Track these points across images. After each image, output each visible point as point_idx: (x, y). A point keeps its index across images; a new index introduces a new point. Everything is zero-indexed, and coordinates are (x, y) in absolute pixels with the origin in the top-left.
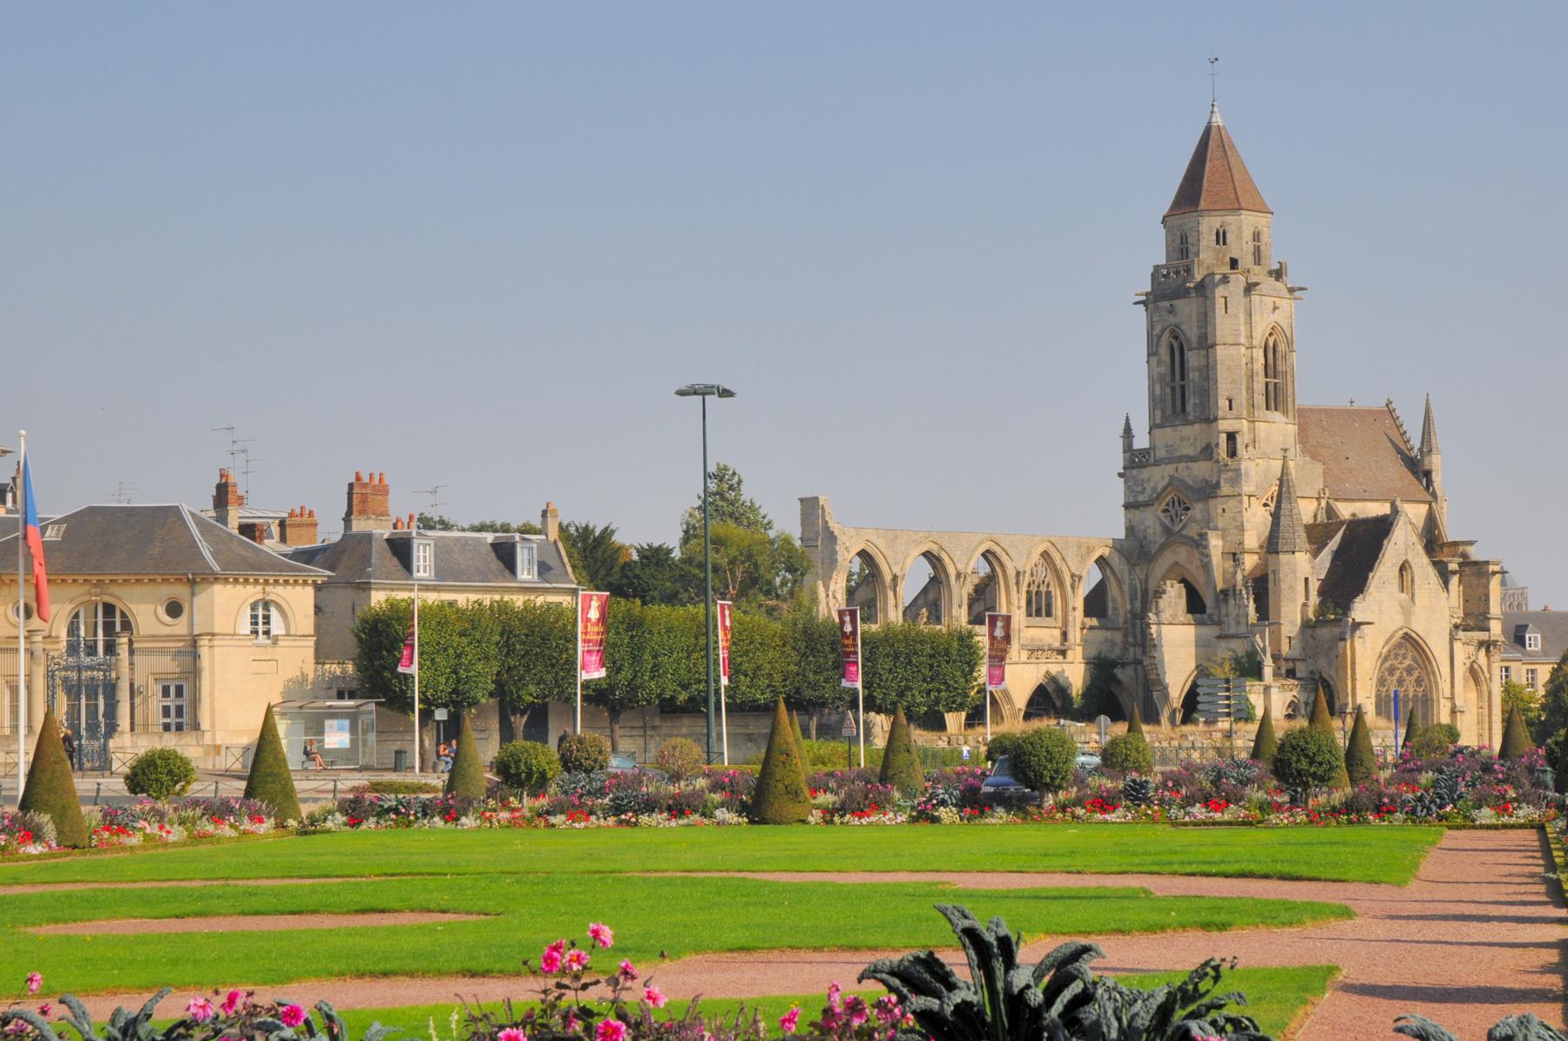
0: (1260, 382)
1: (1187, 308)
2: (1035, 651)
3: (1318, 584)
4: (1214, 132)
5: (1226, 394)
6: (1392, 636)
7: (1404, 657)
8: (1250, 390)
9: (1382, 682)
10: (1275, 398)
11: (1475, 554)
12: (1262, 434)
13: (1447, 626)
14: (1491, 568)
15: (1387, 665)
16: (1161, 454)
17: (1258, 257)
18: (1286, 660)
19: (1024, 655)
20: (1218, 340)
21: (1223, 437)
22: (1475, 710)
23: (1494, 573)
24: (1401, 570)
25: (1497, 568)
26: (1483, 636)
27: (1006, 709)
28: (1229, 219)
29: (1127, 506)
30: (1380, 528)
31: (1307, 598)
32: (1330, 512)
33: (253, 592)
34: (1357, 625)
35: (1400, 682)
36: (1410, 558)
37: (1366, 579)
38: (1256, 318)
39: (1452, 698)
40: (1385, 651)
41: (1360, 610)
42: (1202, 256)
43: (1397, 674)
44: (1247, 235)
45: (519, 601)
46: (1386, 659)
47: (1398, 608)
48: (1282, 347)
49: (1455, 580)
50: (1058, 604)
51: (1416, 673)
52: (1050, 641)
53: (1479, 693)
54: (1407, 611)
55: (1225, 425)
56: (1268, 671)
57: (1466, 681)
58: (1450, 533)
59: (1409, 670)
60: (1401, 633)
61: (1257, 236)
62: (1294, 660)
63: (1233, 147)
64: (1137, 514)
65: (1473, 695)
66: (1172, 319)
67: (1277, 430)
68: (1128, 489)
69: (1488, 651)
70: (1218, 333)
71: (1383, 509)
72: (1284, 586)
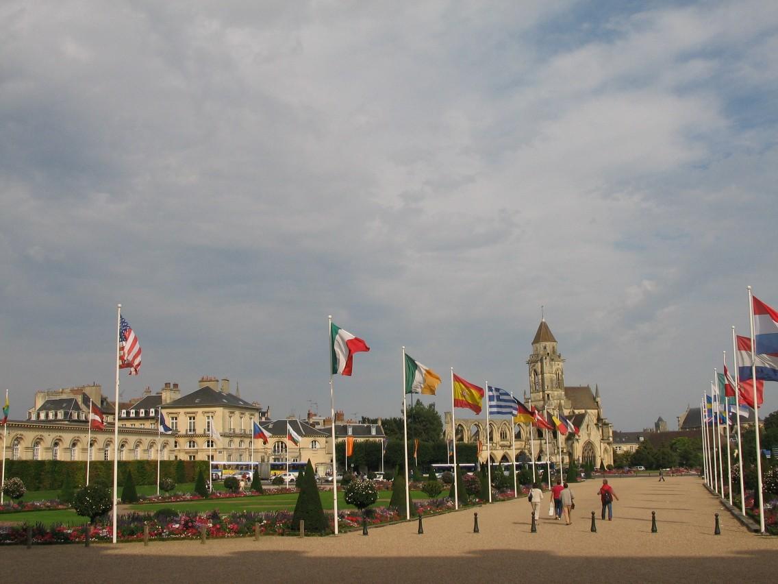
8: (552, 384)
9: (583, 453)
11: (607, 421)
21: (546, 395)
24: (588, 426)
30: (582, 417)
32: (573, 412)
33: (312, 439)
34: (577, 440)
44: (551, 347)
45: (371, 439)
48: (560, 373)
50: (508, 435)
53: (608, 455)
58: (602, 417)
61: (553, 347)
65: (606, 456)
66: (534, 368)
71: (583, 411)
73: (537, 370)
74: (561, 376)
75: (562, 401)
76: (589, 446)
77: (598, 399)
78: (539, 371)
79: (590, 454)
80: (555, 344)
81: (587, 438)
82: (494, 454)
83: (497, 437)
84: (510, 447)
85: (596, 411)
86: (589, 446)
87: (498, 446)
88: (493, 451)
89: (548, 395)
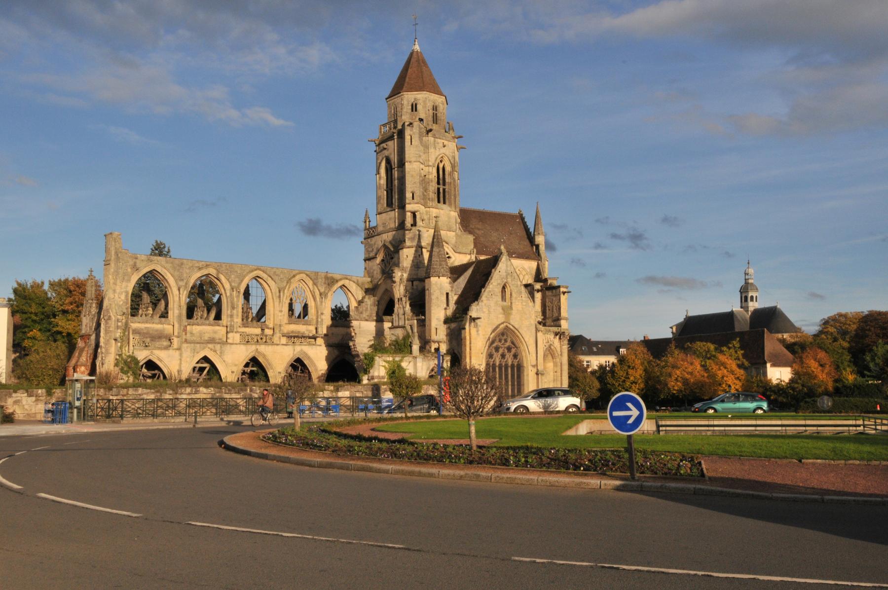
0: (433, 186)
1: (392, 145)
2: (293, 337)
3: (456, 298)
4: (415, 55)
7: (506, 341)
8: (426, 190)
9: (490, 356)
10: (442, 197)
14: (562, 290)
15: (494, 345)
16: (380, 229)
17: (435, 119)
19: (284, 340)
20: (407, 159)
22: (552, 373)
23: (564, 293)
24: (504, 288)
25: (565, 290)
26: (556, 329)
29: (365, 260)
31: (448, 305)
34: (474, 319)
35: (503, 356)
36: (509, 280)
37: (480, 292)
38: (432, 150)
41: (474, 311)
42: (403, 117)
43: (501, 351)
44: (430, 105)
46: (493, 342)
48: (448, 169)
49: (538, 296)
50: (312, 311)
51: (513, 351)
53: (555, 365)
54: (507, 311)
55: (409, 207)
56: (416, 348)
57: (545, 356)
58: (546, 274)
60: (502, 326)
61: (435, 108)
62: (438, 342)
63: (424, 62)
64: (370, 263)
65: (550, 365)
67: (448, 215)
68: (367, 251)
69: (560, 338)
70: (407, 156)
72: (433, 297)
73: (392, 157)
74: (451, 174)
75: (449, 236)
76: (505, 340)
77: (540, 239)
78: (395, 159)
79: (509, 359)
81: (501, 318)
82: (264, 356)
83: (277, 313)
84: (315, 338)
85: (533, 264)
86: (505, 340)
87: (278, 335)
88: (263, 348)
89: (414, 214)
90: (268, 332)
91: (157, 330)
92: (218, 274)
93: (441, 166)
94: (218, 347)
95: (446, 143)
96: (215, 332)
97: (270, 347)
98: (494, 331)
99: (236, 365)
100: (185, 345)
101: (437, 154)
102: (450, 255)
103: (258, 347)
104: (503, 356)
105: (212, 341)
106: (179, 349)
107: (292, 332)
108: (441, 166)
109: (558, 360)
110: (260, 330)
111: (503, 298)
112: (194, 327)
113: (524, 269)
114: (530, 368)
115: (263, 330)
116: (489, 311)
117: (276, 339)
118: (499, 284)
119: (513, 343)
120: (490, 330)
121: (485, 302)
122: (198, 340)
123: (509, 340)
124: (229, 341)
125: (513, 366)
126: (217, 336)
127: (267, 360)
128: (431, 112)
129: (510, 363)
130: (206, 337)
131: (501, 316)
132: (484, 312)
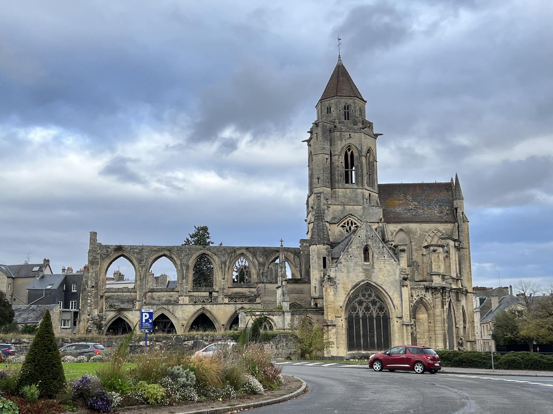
2: (233, 298)
5: (316, 176)
6: (357, 285)
7: (370, 295)
8: (332, 174)
12: (340, 194)
13: (397, 277)
18: (314, 299)
19: (226, 300)
22: (426, 324)
24: (366, 250)
27: (216, 326)
28: (332, 101)
35: (367, 309)
36: (370, 243)
39: (401, 318)
40: (352, 292)
43: (364, 304)
46: (355, 295)
47: (361, 270)
48: (356, 154)
51: (378, 304)
52: (248, 293)
59: (374, 303)
60: (363, 283)
61: (347, 107)
80: (350, 101)
85: (449, 226)
88: (208, 307)
90: (214, 294)
91: (126, 296)
92: (170, 255)
93: (349, 153)
94: (170, 307)
95: (352, 134)
96: (171, 297)
97: (215, 306)
98: (353, 288)
99: (185, 320)
100: (144, 307)
101: (343, 145)
102: (359, 225)
103: (204, 306)
104: (367, 309)
105: (168, 303)
106: (140, 310)
107: (237, 293)
108: (349, 153)
109: (431, 312)
110: (208, 293)
111: (366, 259)
112: (154, 293)
113: (439, 231)
114: (396, 319)
115: (211, 293)
116: (348, 272)
117: (220, 300)
118: (358, 247)
119: (378, 297)
120: (350, 288)
121: (344, 263)
122: (157, 302)
123: (373, 295)
124: (180, 302)
125: (378, 317)
126: (172, 299)
127: (213, 316)
128: (342, 112)
129: (375, 316)
130: (164, 299)
131: (361, 274)
132: (343, 272)
